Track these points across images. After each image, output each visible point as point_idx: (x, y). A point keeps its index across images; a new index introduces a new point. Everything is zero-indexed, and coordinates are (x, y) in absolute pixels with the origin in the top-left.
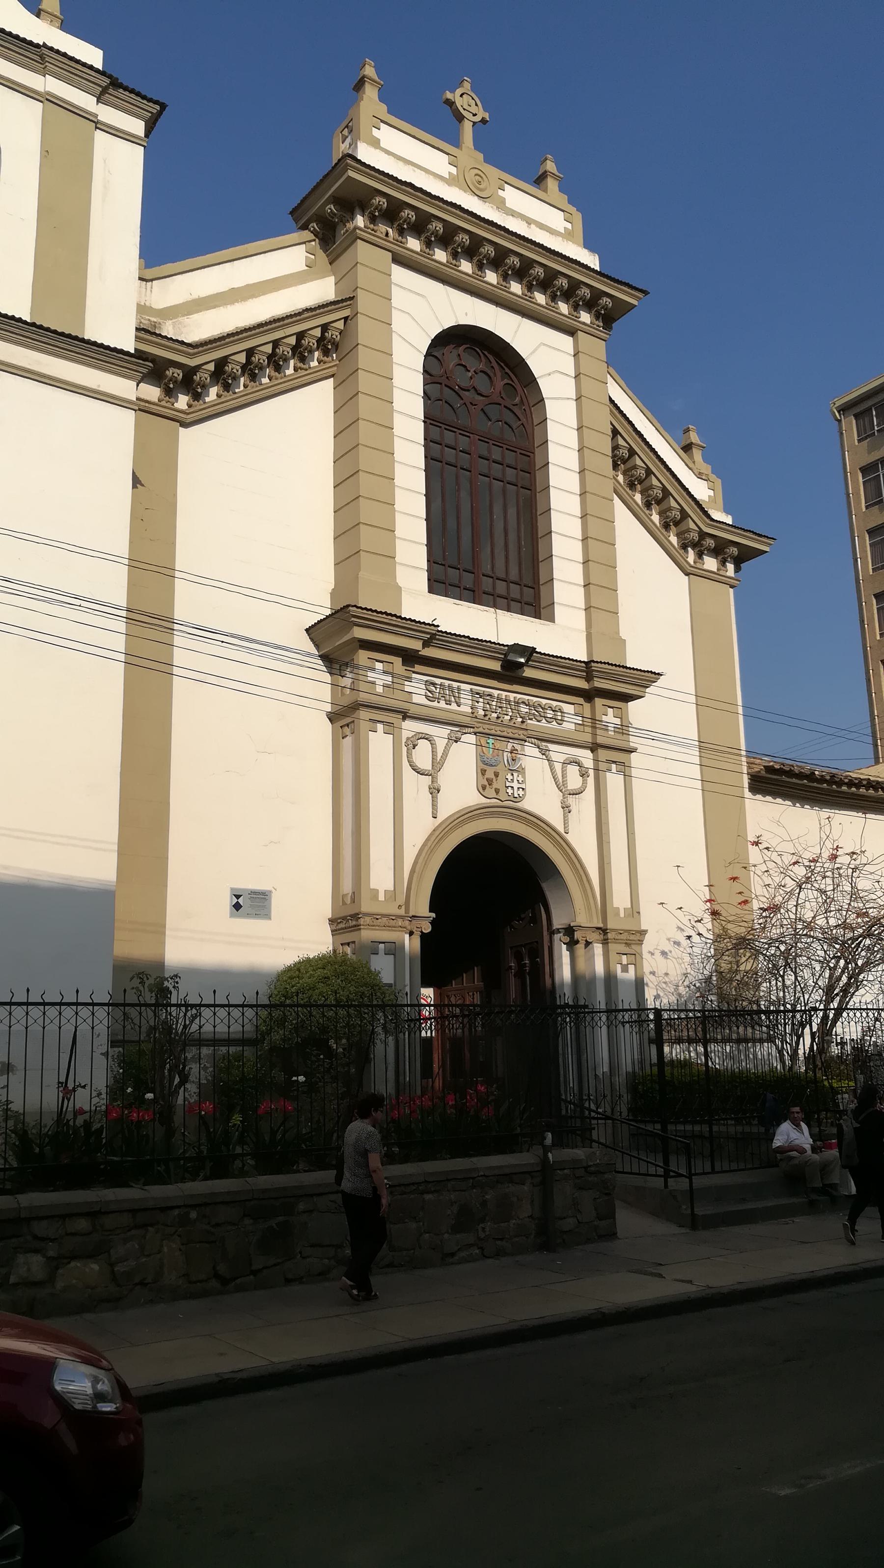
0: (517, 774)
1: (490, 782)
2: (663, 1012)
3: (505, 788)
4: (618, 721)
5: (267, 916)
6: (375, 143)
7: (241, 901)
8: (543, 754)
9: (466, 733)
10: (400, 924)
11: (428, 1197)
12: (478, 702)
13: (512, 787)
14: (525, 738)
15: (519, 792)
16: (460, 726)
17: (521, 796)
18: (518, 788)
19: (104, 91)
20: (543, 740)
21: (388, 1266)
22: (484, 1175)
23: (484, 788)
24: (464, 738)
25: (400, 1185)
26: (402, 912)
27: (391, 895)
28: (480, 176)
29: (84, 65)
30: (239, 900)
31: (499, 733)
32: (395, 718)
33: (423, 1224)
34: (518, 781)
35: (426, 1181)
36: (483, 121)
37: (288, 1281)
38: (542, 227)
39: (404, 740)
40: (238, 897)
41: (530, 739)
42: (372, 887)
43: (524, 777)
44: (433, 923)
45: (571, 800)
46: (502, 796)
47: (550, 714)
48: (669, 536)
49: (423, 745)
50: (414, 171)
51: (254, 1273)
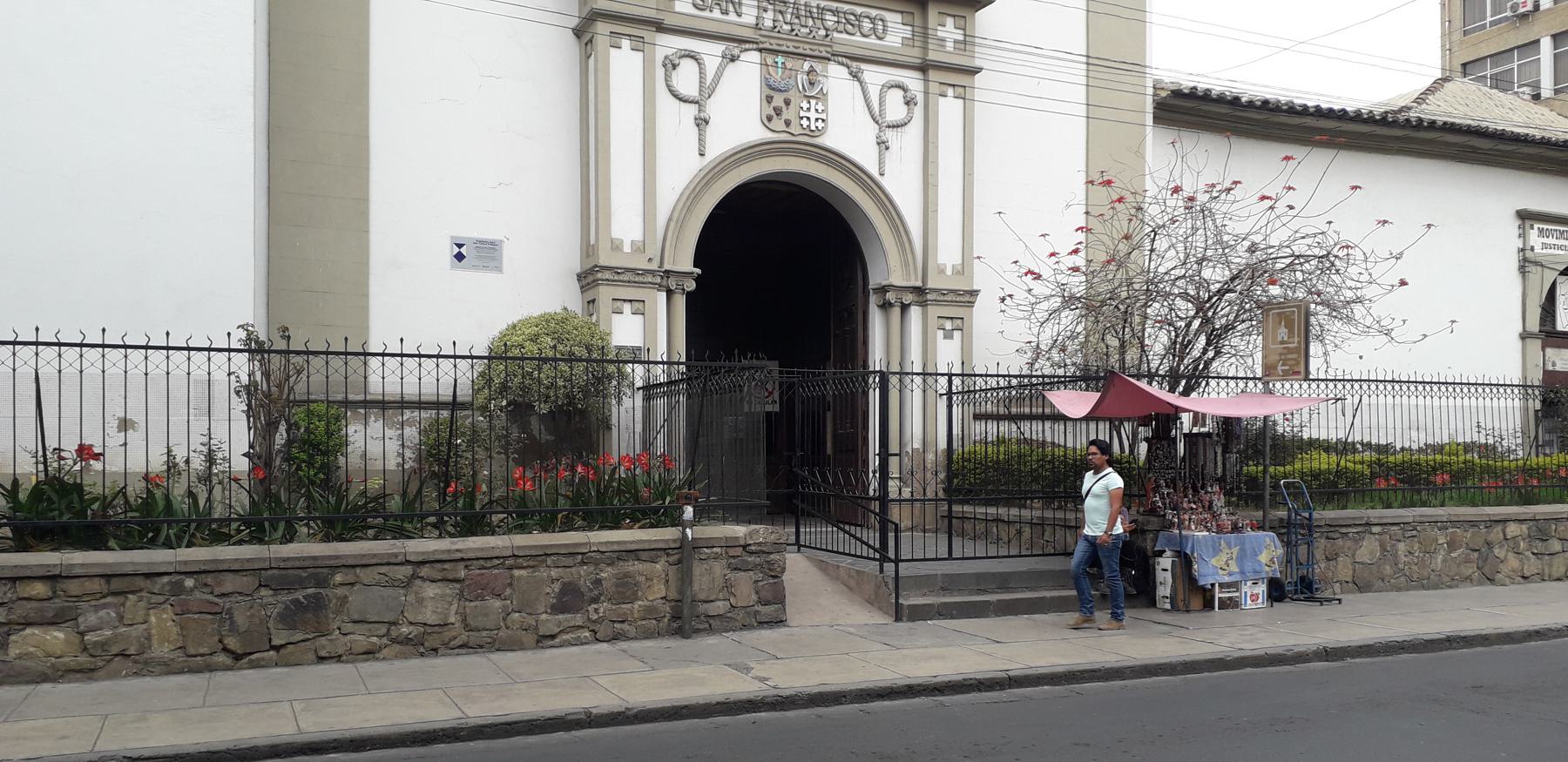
1: (778, 111)
2: (890, 376)
3: (798, 119)
5: (499, 269)
7: (463, 250)
8: (854, 77)
10: (650, 280)
11: (516, 573)
12: (765, 10)
13: (808, 119)
14: (829, 56)
15: (817, 124)
16: (736, 42)
17: (820, 128)
18: (817, 120)
20: (854, 60)
21: (460, 647)
22: (598, 551)
23: (770, 119)
24: (744, 56)
25: (477, 559)
26: (654, 266)
27: (639, 248)
30: (461, 250)
31: (791, 49)
33: (512, 602)
34: (817, 110)
35: (514, 556)
37: (321, 659)
39: (659, 59)
40: (460, 246)
41: (836, 58)
42: (615, 234)
43: (826, 105)
44: (698, 279)
45: (890, 135)
46: (794, 129)
47: (867, 25)
49: (688, 66)
51: (277, 648)
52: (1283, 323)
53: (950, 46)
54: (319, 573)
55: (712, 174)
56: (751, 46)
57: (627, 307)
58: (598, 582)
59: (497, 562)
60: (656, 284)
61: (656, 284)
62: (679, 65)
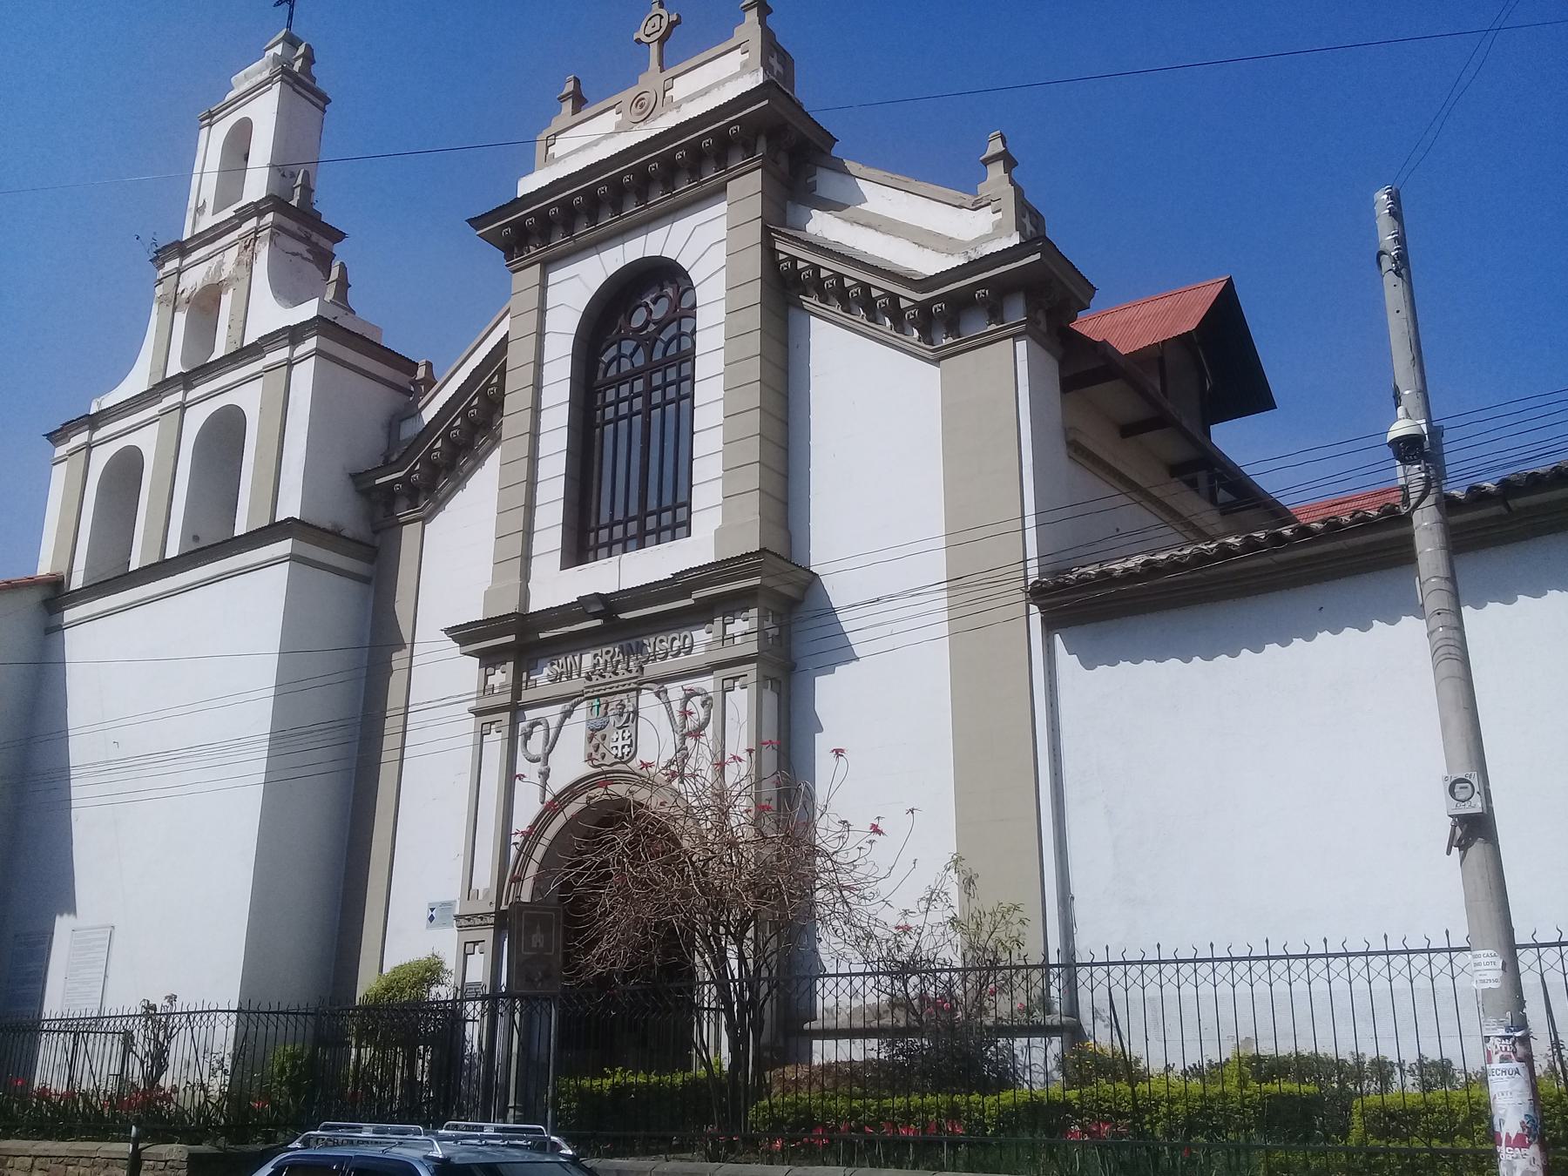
0: (621, 731)
1: (597, 748)
6: (549, 160)
13: (617, 748)
14: (635, 686)
16: (570, 701)
18: (623, 747)
23: (590, 758)
28: (643, 99)
32: (506, 716)
34: (623, 739)
36: (672, 25)
41: (645, 686)
46: (609, 759)
47: (677, 644)
50: (565, 162)
52: (538, 927)
56: (579, 698)
59: (62, 1159)
60: (491, 924)
61: (491, 924)
62: (531, 733)
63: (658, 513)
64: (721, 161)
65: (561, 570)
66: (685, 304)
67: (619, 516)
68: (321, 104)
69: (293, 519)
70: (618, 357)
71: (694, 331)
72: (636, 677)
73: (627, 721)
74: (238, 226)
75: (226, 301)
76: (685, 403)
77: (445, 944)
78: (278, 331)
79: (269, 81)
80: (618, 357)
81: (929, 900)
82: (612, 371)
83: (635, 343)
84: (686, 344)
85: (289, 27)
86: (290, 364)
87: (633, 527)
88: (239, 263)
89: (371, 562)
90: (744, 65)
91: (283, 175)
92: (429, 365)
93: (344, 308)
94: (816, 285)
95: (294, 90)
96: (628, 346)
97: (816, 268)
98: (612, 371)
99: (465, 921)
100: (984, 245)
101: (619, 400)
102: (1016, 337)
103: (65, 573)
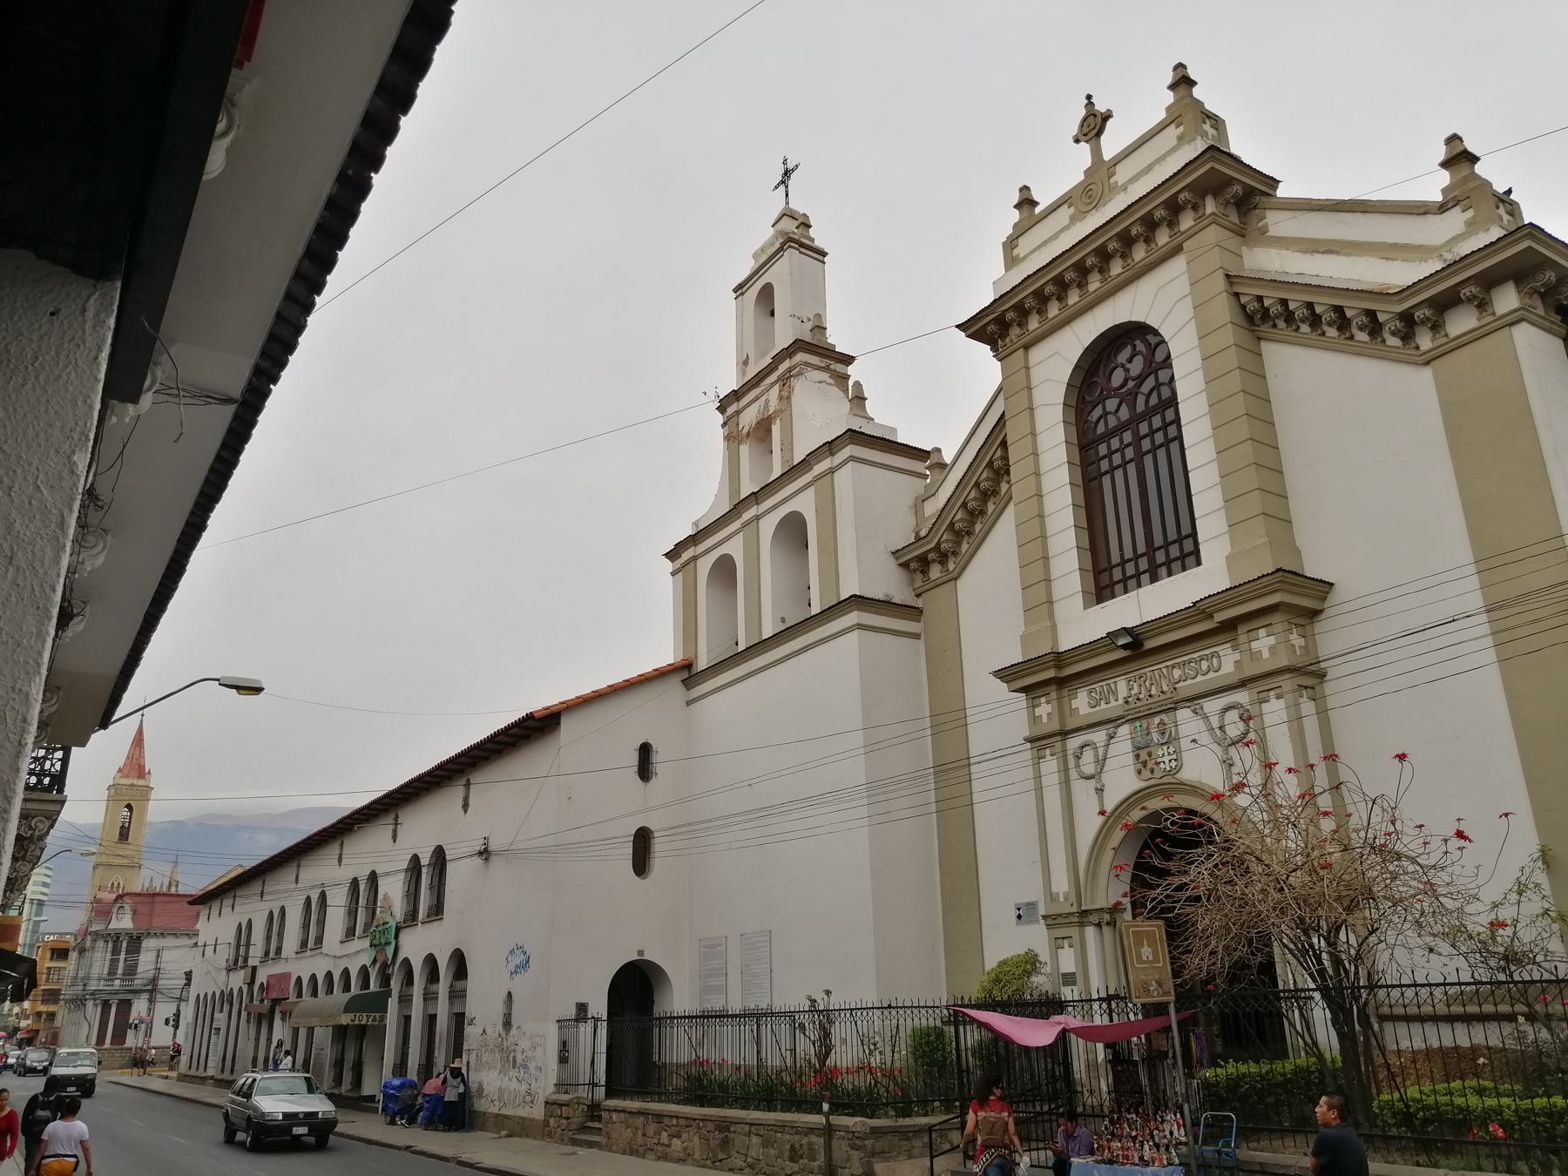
1: (1145, 764)
4: (1272, 640)
7: (1021, 912)
9: (1119, 726)
14: (1173, 705)
18: (1170, 761)
19: (830, 449)
23: (1139, 772)
26: (1075, 909)
28: (1091, 190)
29: (818, 449)
38: (1149, 168)
40: (1019, 909)
46: (1158, 774)
47: (1205, 665)
48: (1384, 341)
52: (1145, 942)
53: (1266, 654)
54: (724, 1126)
55: (1106, 828)
56: (1121, 721)
57: (1065, 941)
58: (801, 1145)
63: (1167, 545)
64: (1172, 223)
65: (1084, 609)
66: (1159, 356)
67: (1129, 554)
68: (821, 258)
69: (855, 596)
70: (1105, 414)
71: (1172, 378)
72: (1172, 698)
73: (1169, 738)
74: (776, 368)
75: (776, 429)
76: (1174, 446)
77: (1036, 938)
78: (820, 447)
79: (781, 249)
80: (1105, 414)
81: (1520, 893)
82: (1101, 429)
83: (1117, 401)
84: (1165, 393)
85: (787, 203)
86: (832, 471)
87: (1143, 564)
88: (781, 398)
89: (919, 621)
90: (1180, 138)
91: (802, 322)
92: (938, 450)
93: (867, 418)
94: (1289, 317)
95: (801, 252)
96: (1111, 404)
97: (1284, 302)
98: (1101, 429)
99: (1052, 921)
100: (1459, 245)
101: (1111, 453)
102: (1511, 325)
103: (694, 657)
